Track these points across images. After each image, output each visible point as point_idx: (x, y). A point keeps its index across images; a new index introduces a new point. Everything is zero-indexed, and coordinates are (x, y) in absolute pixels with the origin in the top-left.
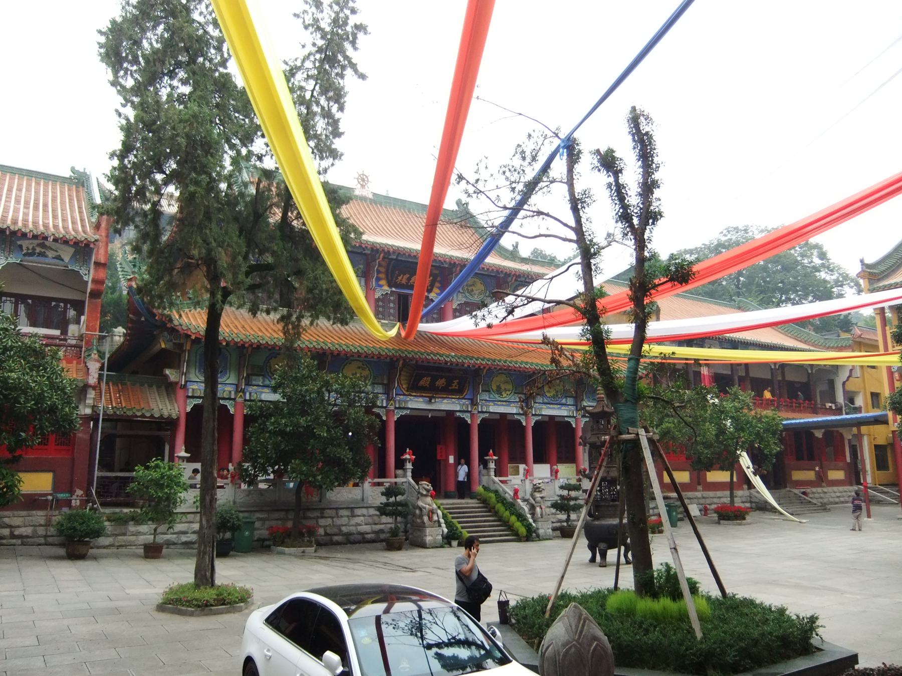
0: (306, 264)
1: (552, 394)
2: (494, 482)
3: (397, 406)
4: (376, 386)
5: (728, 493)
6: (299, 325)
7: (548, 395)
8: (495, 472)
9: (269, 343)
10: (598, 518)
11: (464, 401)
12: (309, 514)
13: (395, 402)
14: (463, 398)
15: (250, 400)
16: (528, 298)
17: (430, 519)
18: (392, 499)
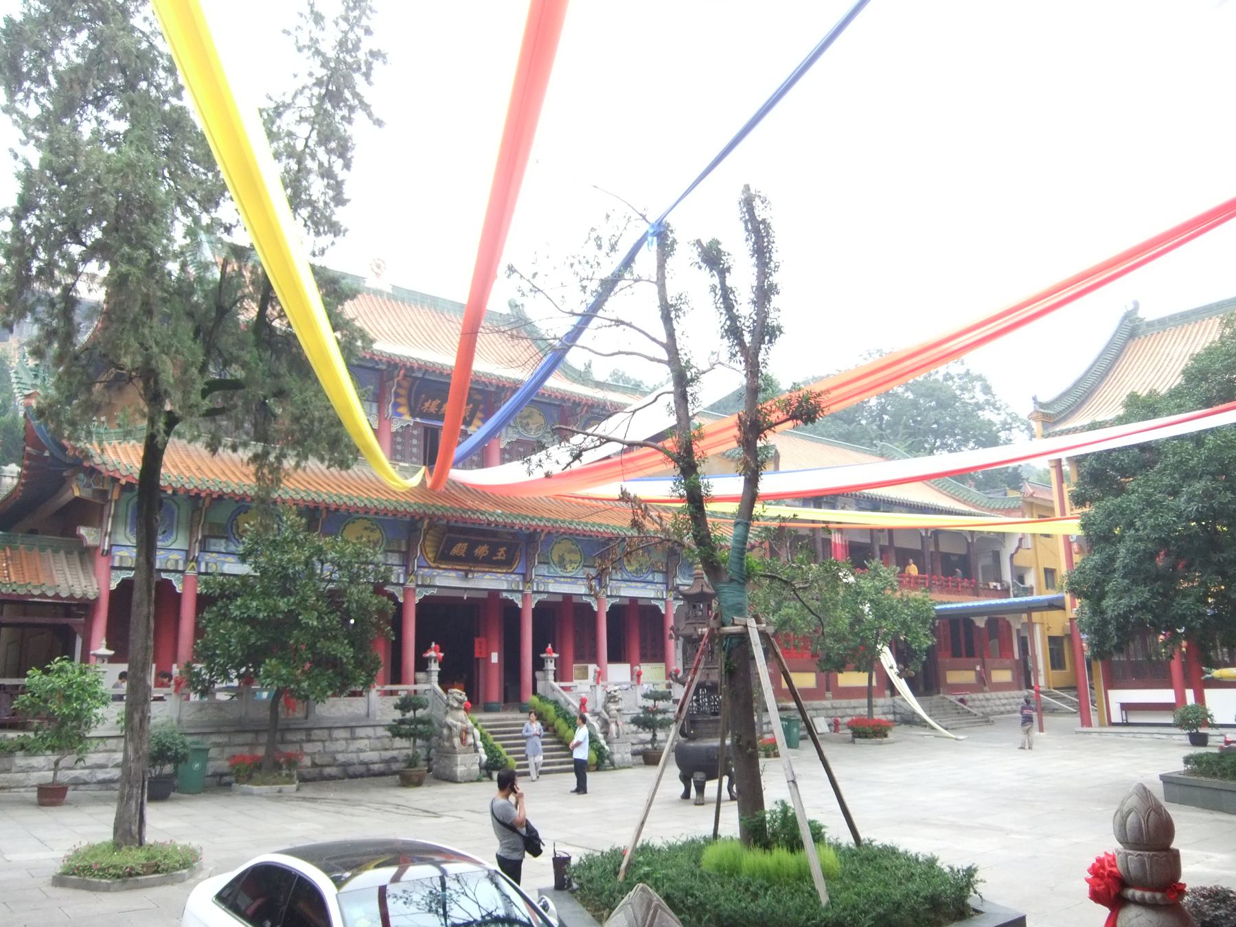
0: (291, 382)
1: (634, 568)
2: (553, 689)
3: (420, 583)
4: (389, 554)
5: (865, 701)
6: (278, 469)
7: (629, 569)
8: (555, 675)
9: (237, 491)
10: (693, 738)
11: (513, 576)
12: (290, 736)
13: (416, 577)
14: (512, 573)
15: (206, 574)
16: (601, 437)
17: (463, 741)
18: (410, 715)
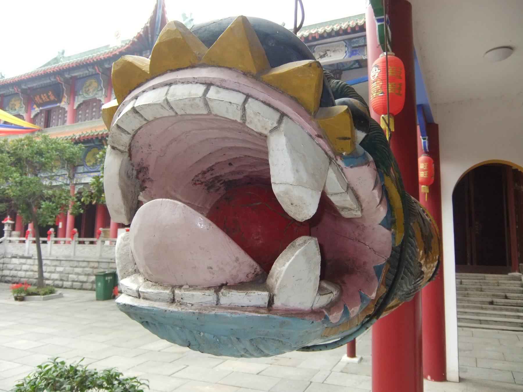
1: (91, 163)
